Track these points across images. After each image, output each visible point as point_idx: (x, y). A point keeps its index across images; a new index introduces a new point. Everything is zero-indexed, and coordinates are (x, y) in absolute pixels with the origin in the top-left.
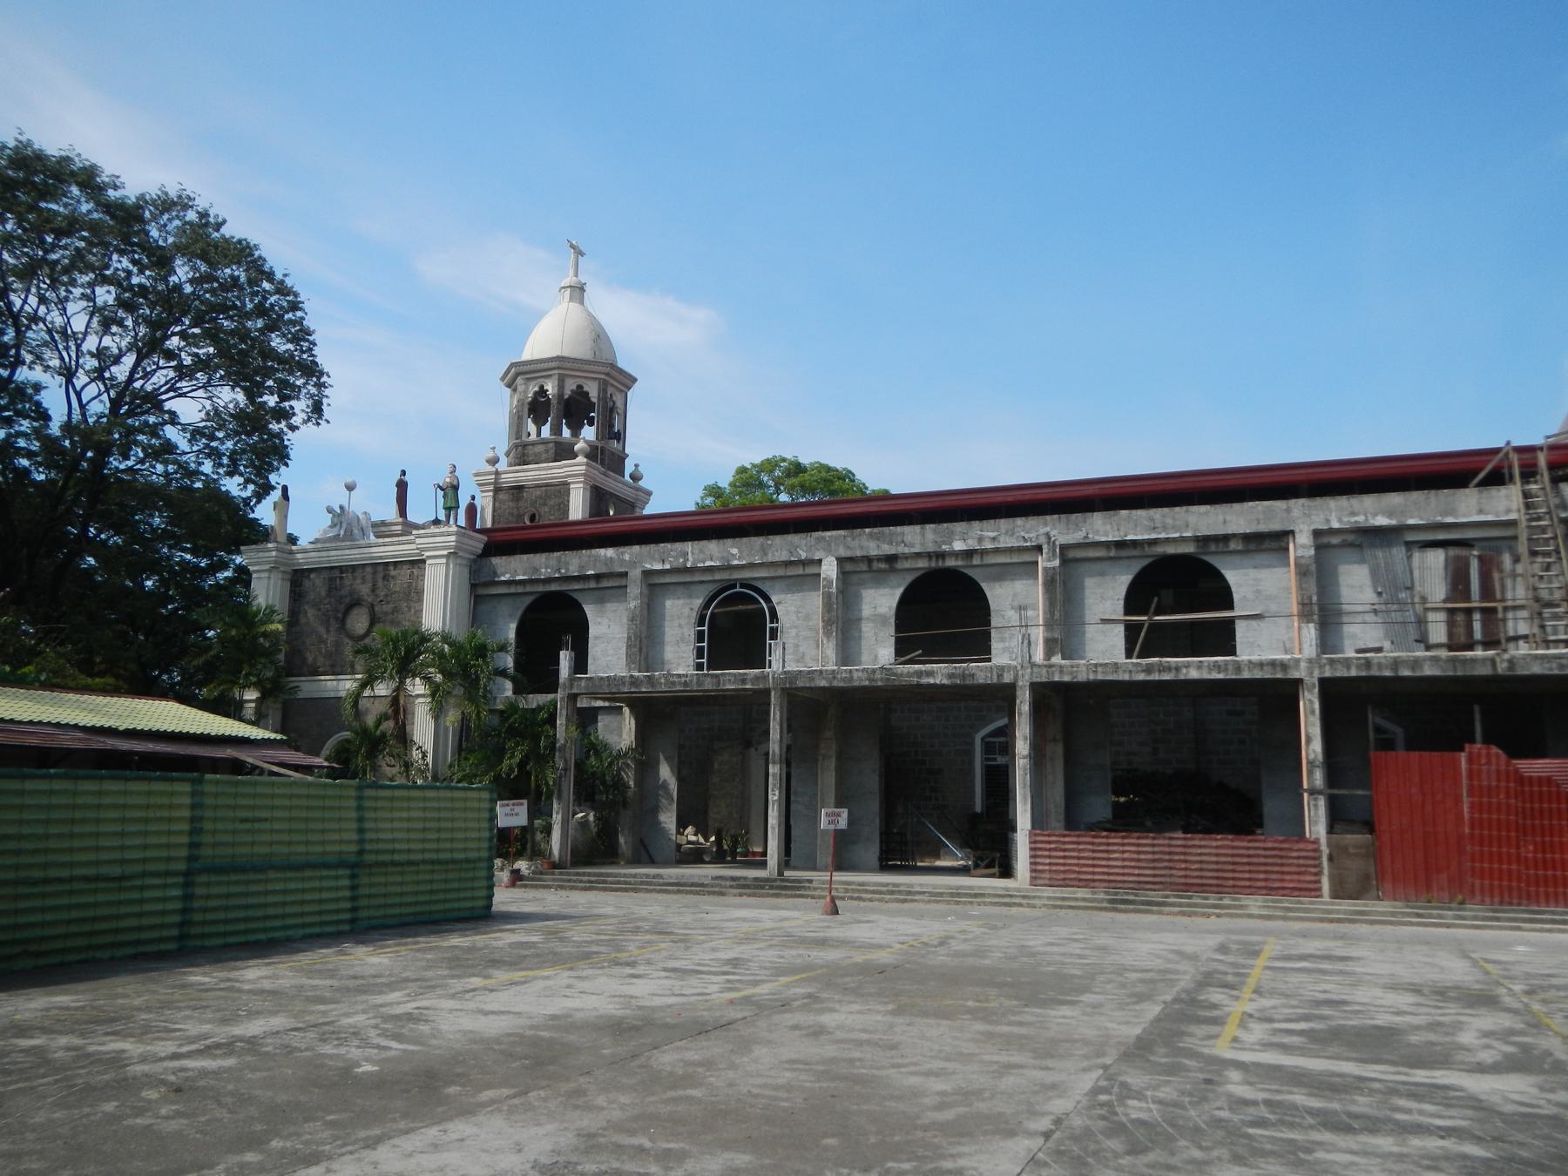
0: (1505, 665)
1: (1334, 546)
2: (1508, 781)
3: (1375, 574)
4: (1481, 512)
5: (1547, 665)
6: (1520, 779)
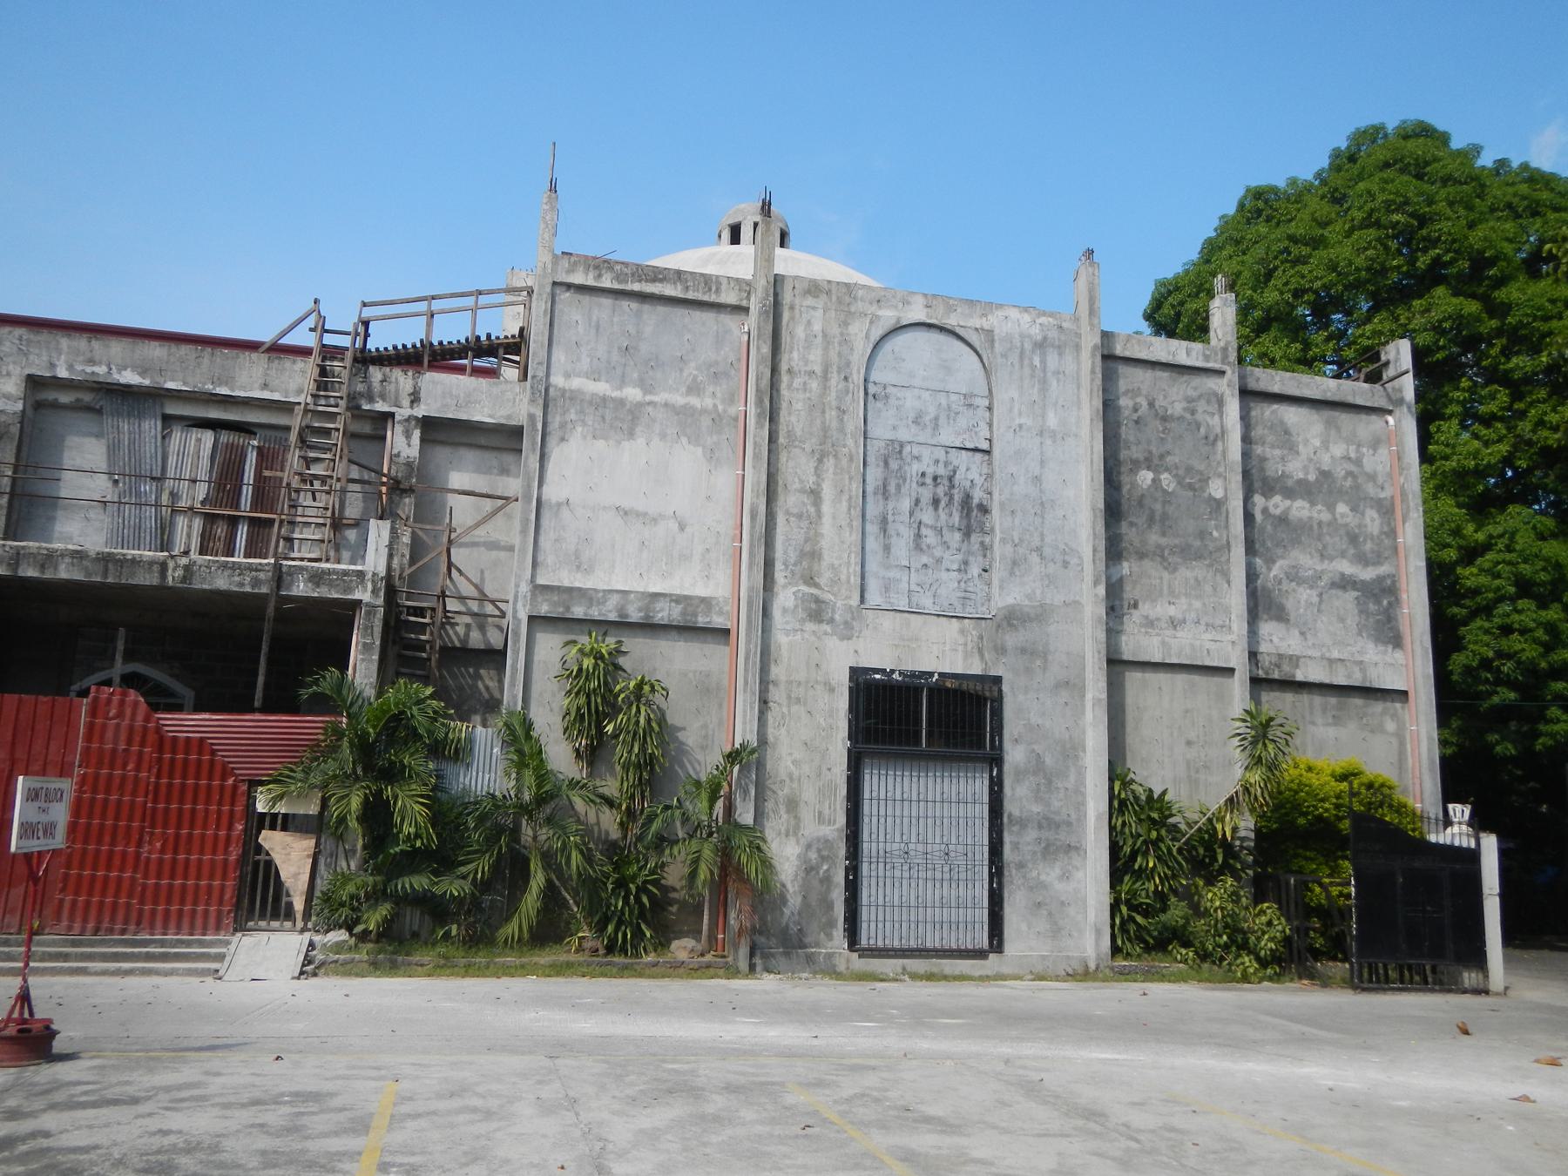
0: (179, 573)
1: (64, 407)
2: (143, 744)
3: (113, 450)
4: (265, 386)
5: (237, 579)
6: (161, 741)
